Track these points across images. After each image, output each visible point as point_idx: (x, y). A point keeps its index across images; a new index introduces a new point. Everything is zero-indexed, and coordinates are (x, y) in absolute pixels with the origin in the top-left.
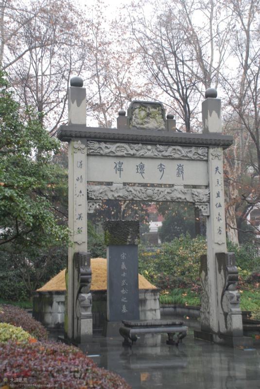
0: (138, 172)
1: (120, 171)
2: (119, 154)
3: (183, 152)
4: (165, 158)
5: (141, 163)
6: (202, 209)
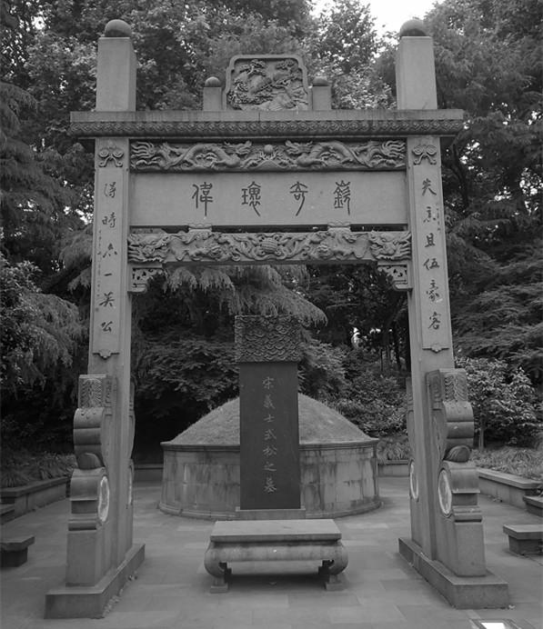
0: (245, 203)
1: (206, 201)
2: (201, 165)
3: (346, 152)
4: (308, 169)
5: (253, 183)
6: (395, 277)
